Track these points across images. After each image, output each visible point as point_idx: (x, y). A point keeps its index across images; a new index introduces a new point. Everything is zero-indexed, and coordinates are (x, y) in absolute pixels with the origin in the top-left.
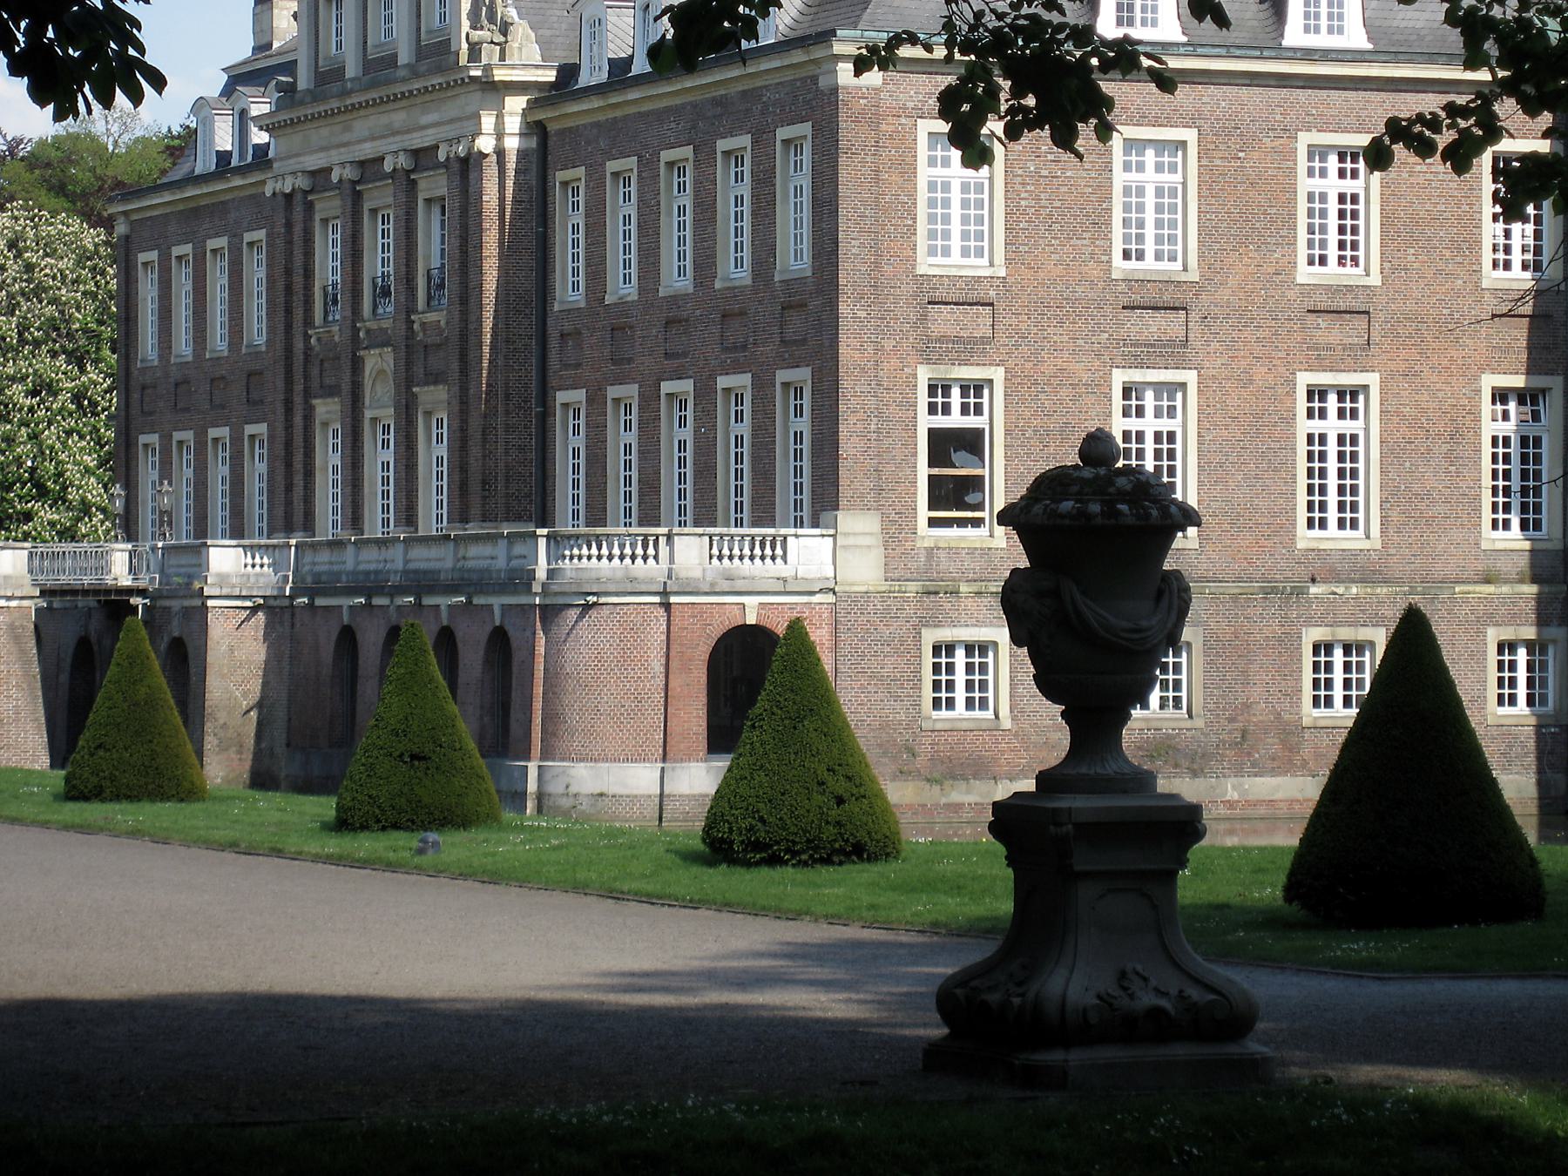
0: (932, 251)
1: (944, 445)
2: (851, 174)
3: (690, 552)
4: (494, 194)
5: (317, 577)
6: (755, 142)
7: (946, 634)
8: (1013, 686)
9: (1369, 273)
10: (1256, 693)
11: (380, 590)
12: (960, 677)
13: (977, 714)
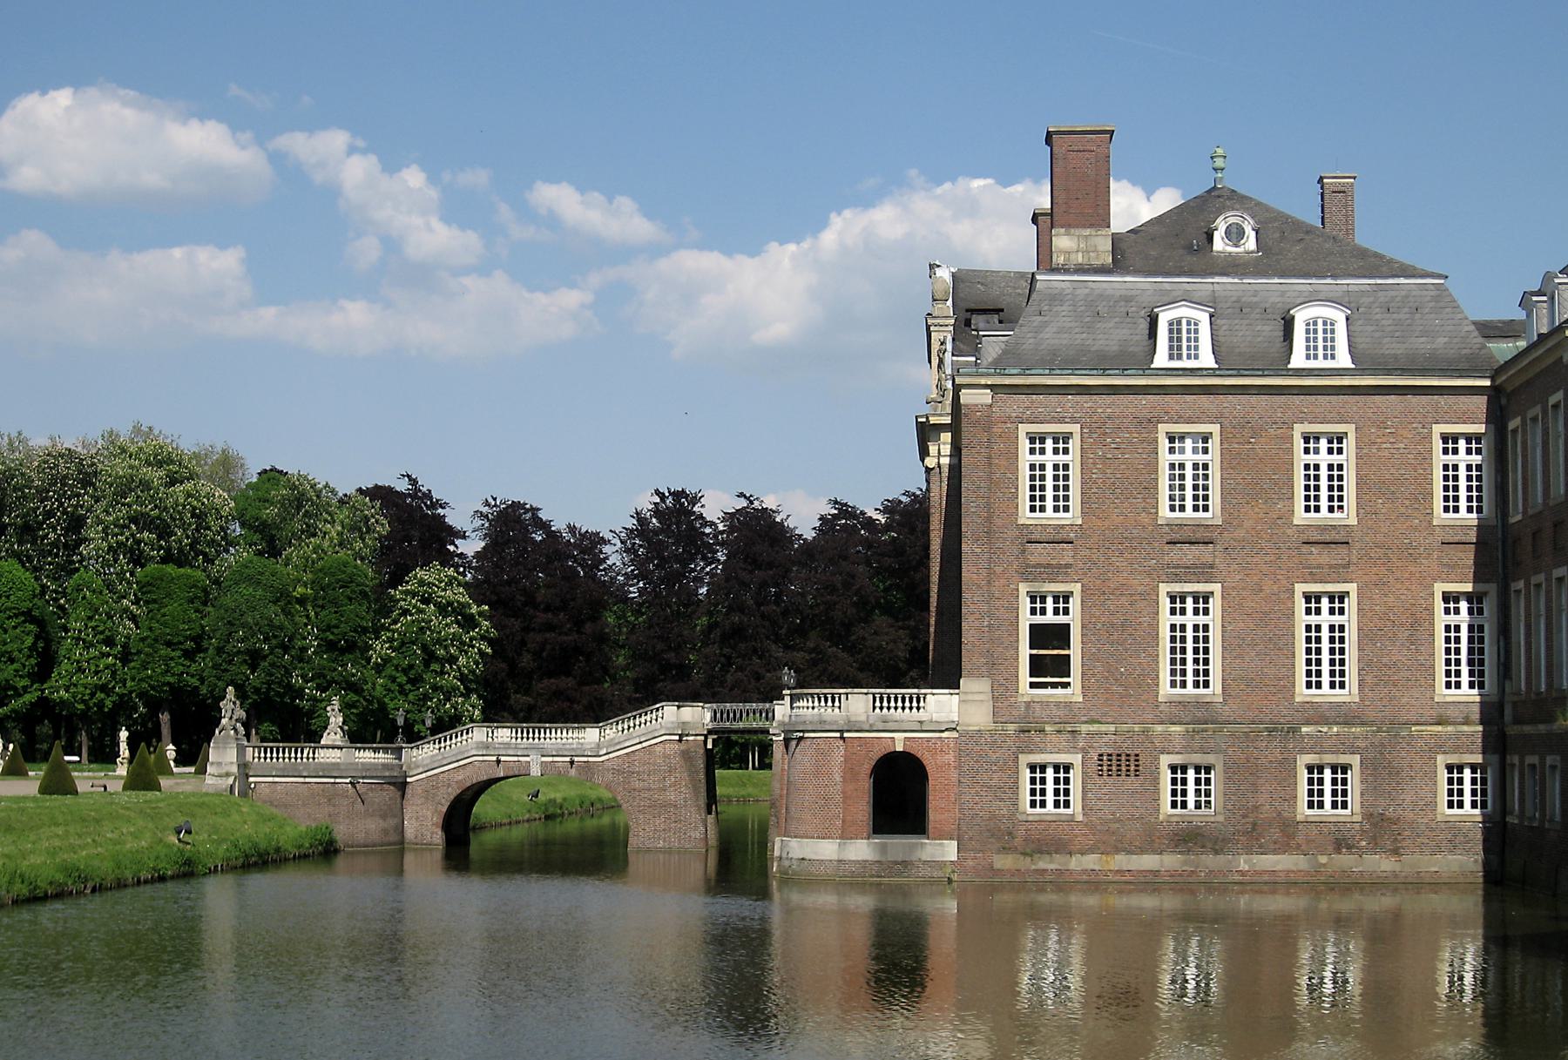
1: (1040, 635)
3: (857, 704)
7: (1038, 758)
9: (1349, 516)
10: (1263, 798)
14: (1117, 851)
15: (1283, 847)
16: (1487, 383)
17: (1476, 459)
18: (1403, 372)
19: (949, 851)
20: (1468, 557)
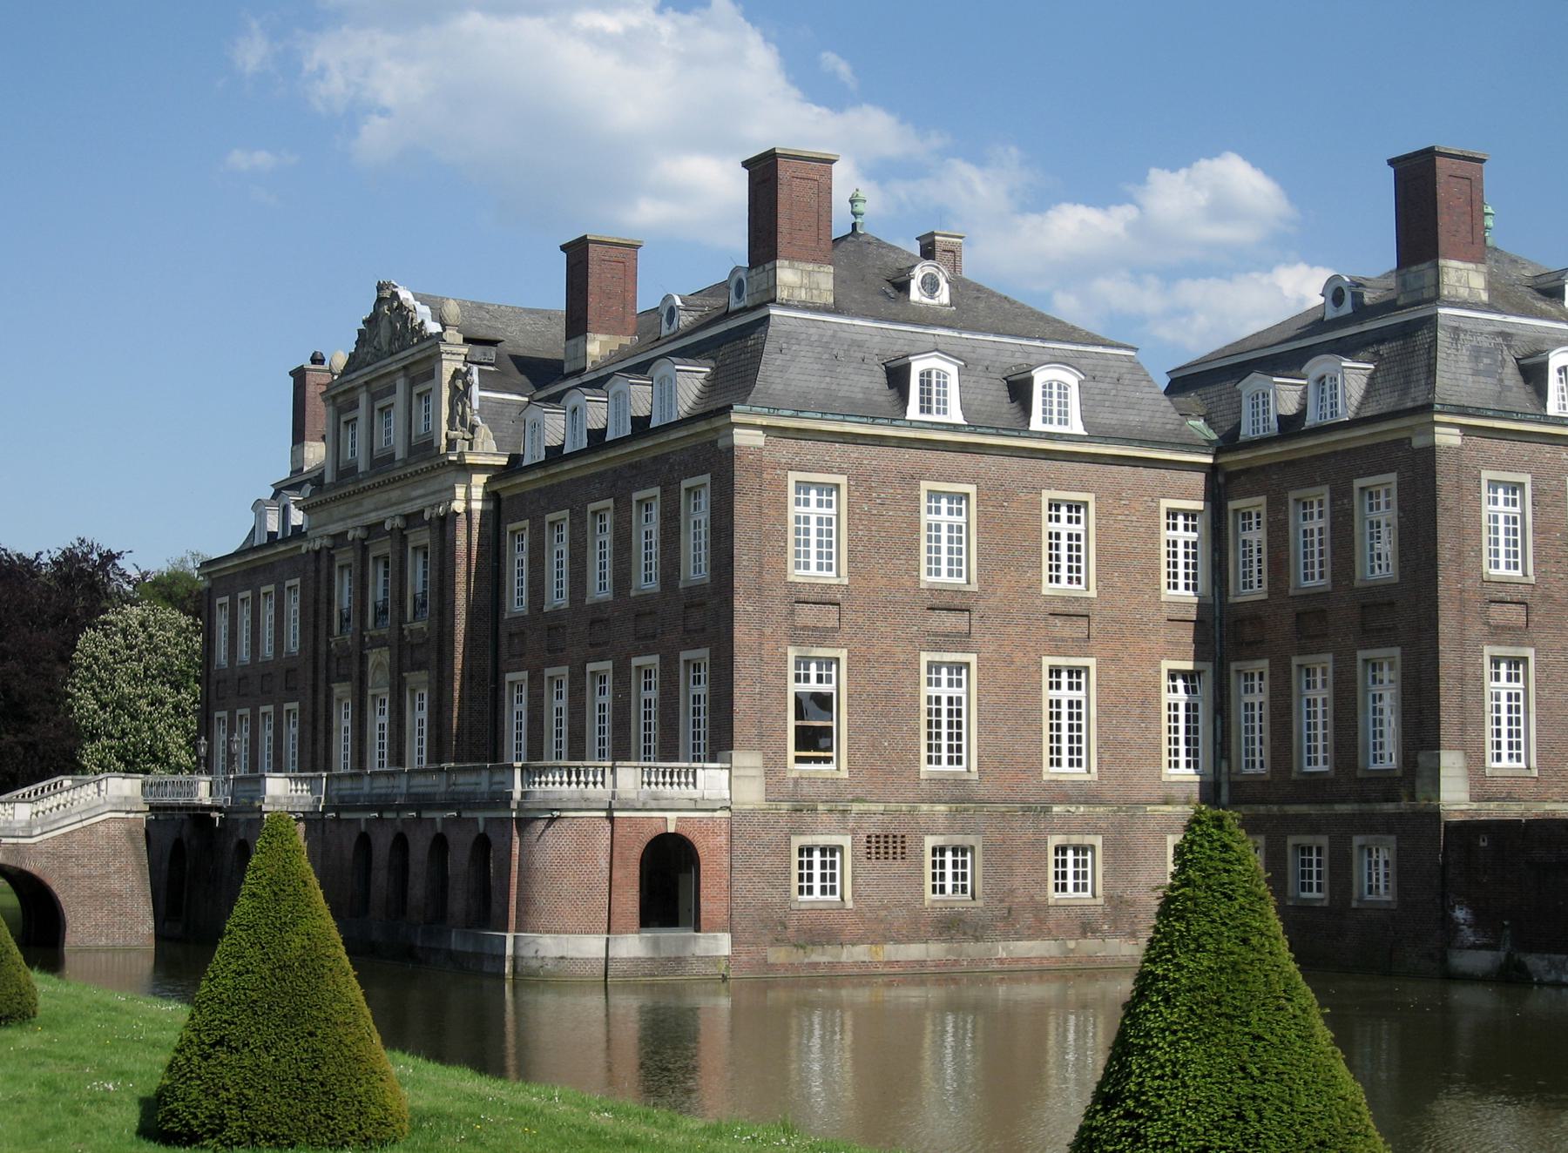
0: (797, 565)
2: (743, 507)
3: (629, 779)
4: (465, 541)
5: (342, 798)
6: (663, 492)
7: (807, 840)
8: (854, 878)
11: (389, 807)
12: (817, 871)
13: (828, 897)
14: (886, 939)
15: (1038, 930)
16: (1209, 460)
17: (1192, 536)
18: (1142, 443)
19: (721, 944)
20: (1187, 635)
